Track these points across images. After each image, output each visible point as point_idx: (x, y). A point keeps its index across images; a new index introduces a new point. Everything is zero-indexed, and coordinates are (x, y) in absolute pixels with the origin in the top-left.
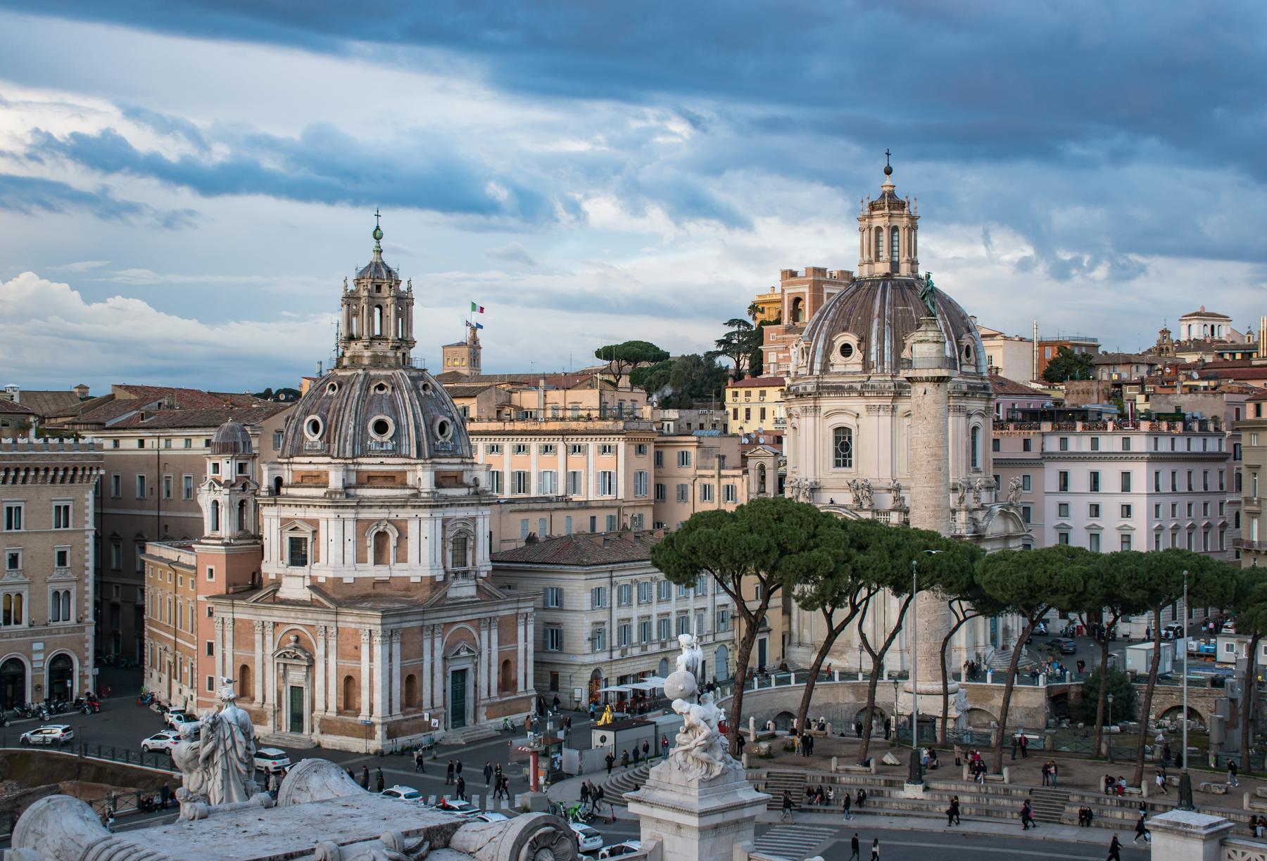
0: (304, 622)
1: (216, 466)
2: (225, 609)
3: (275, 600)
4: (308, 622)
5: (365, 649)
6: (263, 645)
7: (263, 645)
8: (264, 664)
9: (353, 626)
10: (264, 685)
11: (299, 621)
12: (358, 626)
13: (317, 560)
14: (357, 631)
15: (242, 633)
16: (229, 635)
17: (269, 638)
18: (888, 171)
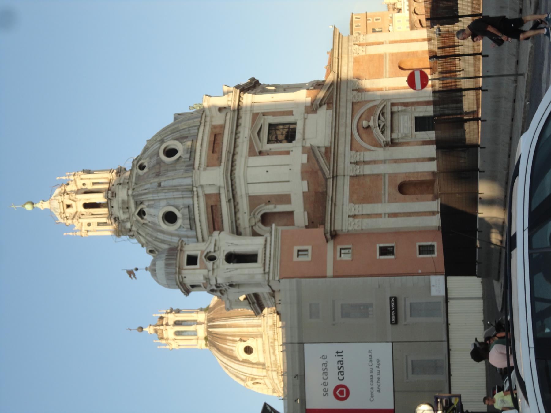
0: (349, 116)
1: (192, 260)
2: (338, 217)
3: (330, 153)
4: (349, 111)
5: (373, 50)
6: (375, 162)
7: (375, 162)
8: (396, 161)
9: (351, 65)
10: (418, 160)
11: (349, 121)
12: (351, 60)
13: (291, 113)
14: (357, 61)
15: (365, 189)
16: (368, 208)
17: (368, 156)
18: (141, 329)
